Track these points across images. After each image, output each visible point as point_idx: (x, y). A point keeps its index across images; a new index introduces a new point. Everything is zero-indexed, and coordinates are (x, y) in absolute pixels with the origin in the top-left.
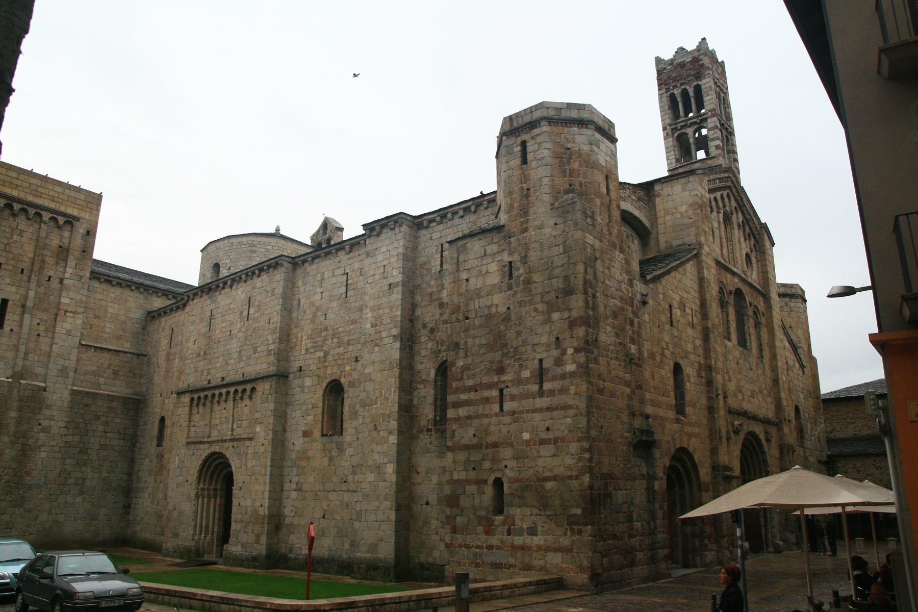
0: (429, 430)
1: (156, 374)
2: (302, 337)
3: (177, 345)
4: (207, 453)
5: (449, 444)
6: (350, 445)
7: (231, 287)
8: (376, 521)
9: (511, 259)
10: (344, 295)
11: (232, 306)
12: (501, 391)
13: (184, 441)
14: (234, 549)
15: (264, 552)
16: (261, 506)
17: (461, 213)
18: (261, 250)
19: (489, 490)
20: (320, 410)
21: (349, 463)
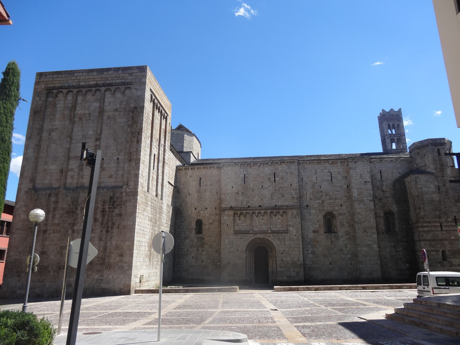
0: (383, 233)
1: (188, 198)
2: (306, 193)
3: (206, 185)
4: (253, 238)
5: (422, 239)
6: (342, 237)
7: (259, 166)
8: (371, 264)
9: (439, 184)
10: (331, 180)
11: (261, 175)
12: (441, 224)
13: (232, 232)
14: (280, 279)
15: (304, 279)
16: (298, 260)
17: (389, 161)
18: (188, 139)
19: (440, 253)
20: (322, 223)
21: (342, 244)
